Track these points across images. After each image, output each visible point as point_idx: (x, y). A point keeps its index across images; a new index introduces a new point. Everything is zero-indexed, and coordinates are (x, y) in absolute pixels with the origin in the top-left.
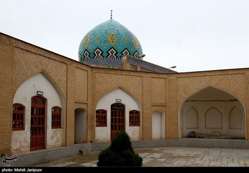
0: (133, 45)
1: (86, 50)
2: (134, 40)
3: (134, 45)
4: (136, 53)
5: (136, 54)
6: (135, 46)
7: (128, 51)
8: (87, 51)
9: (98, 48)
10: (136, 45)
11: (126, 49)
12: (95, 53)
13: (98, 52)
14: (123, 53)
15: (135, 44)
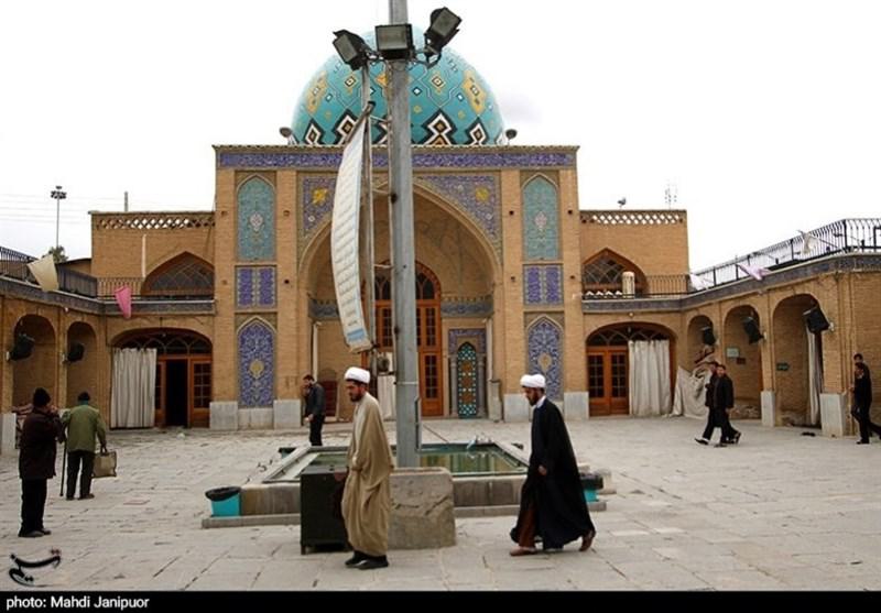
0: (465, 101)
1: (313, 122)
2: (470, 84)
3: (469, 102)
4: (479, 126)
5: (475, 129)
6: (474, 104)
7: (446, 118)
8: (316, 126)
9: (348, 112)
10: (477, 102)
11: (440, 111)
12: (339, 129)
13: (348, 127)
14: (430, 126)
15: (474, 97)
